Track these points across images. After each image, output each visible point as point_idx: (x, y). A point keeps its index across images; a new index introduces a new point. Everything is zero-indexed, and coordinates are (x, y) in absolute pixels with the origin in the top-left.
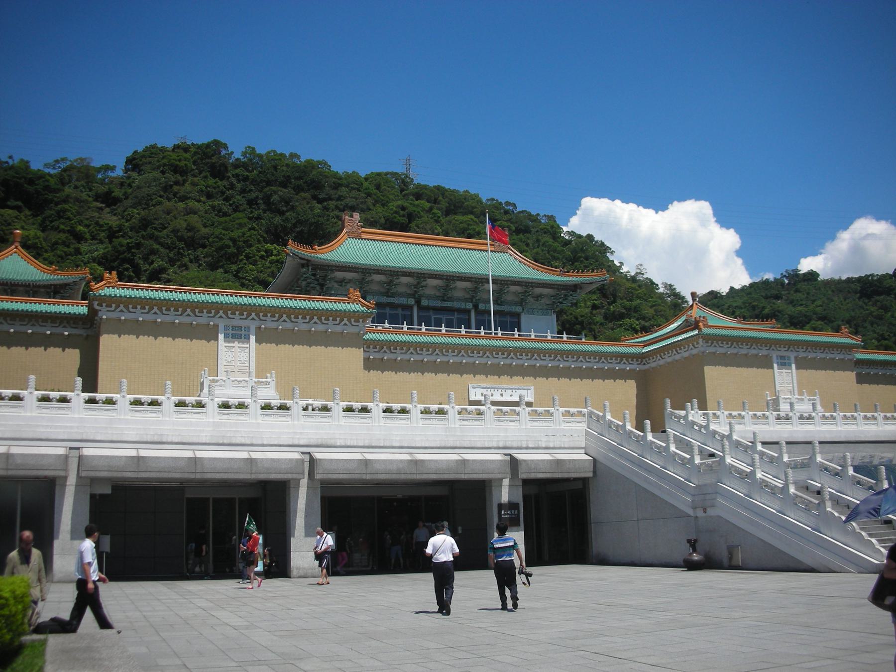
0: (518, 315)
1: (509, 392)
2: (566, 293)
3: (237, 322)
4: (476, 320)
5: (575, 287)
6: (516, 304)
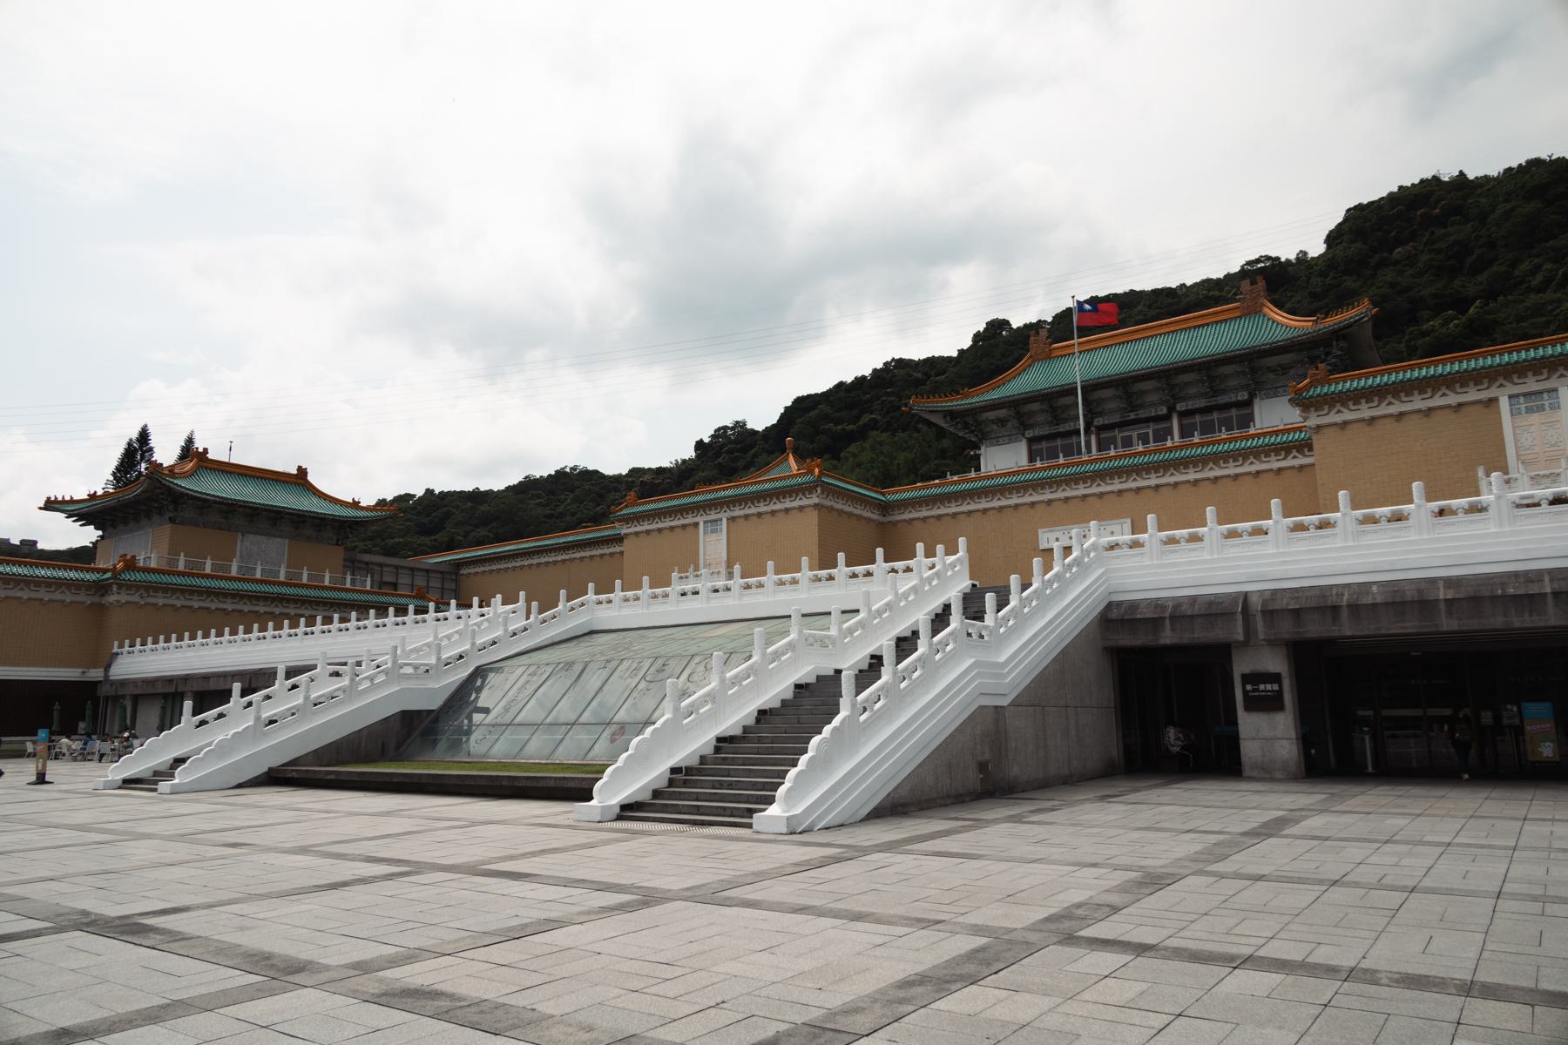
0: (1249, 404)
3: (713, 517)
6: (1243, 387)
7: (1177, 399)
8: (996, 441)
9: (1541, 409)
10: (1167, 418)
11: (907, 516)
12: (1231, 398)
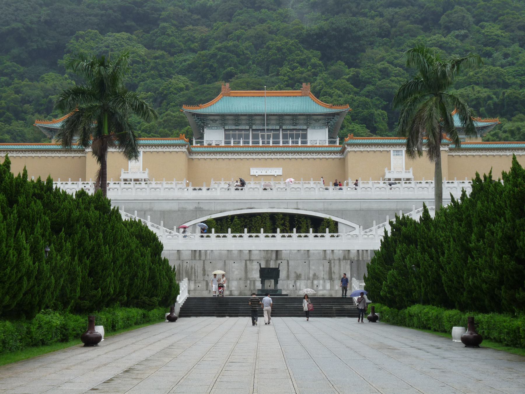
0: (306, 130)
1: (270, 171)
2: (330, 117)
4: (283, 135)
5: (333, 115)
7: (283, 124)
8: (211, 128)
9: (399, 155)
10: (279, 130)
11: (199, 157)
12: (301, 127)
